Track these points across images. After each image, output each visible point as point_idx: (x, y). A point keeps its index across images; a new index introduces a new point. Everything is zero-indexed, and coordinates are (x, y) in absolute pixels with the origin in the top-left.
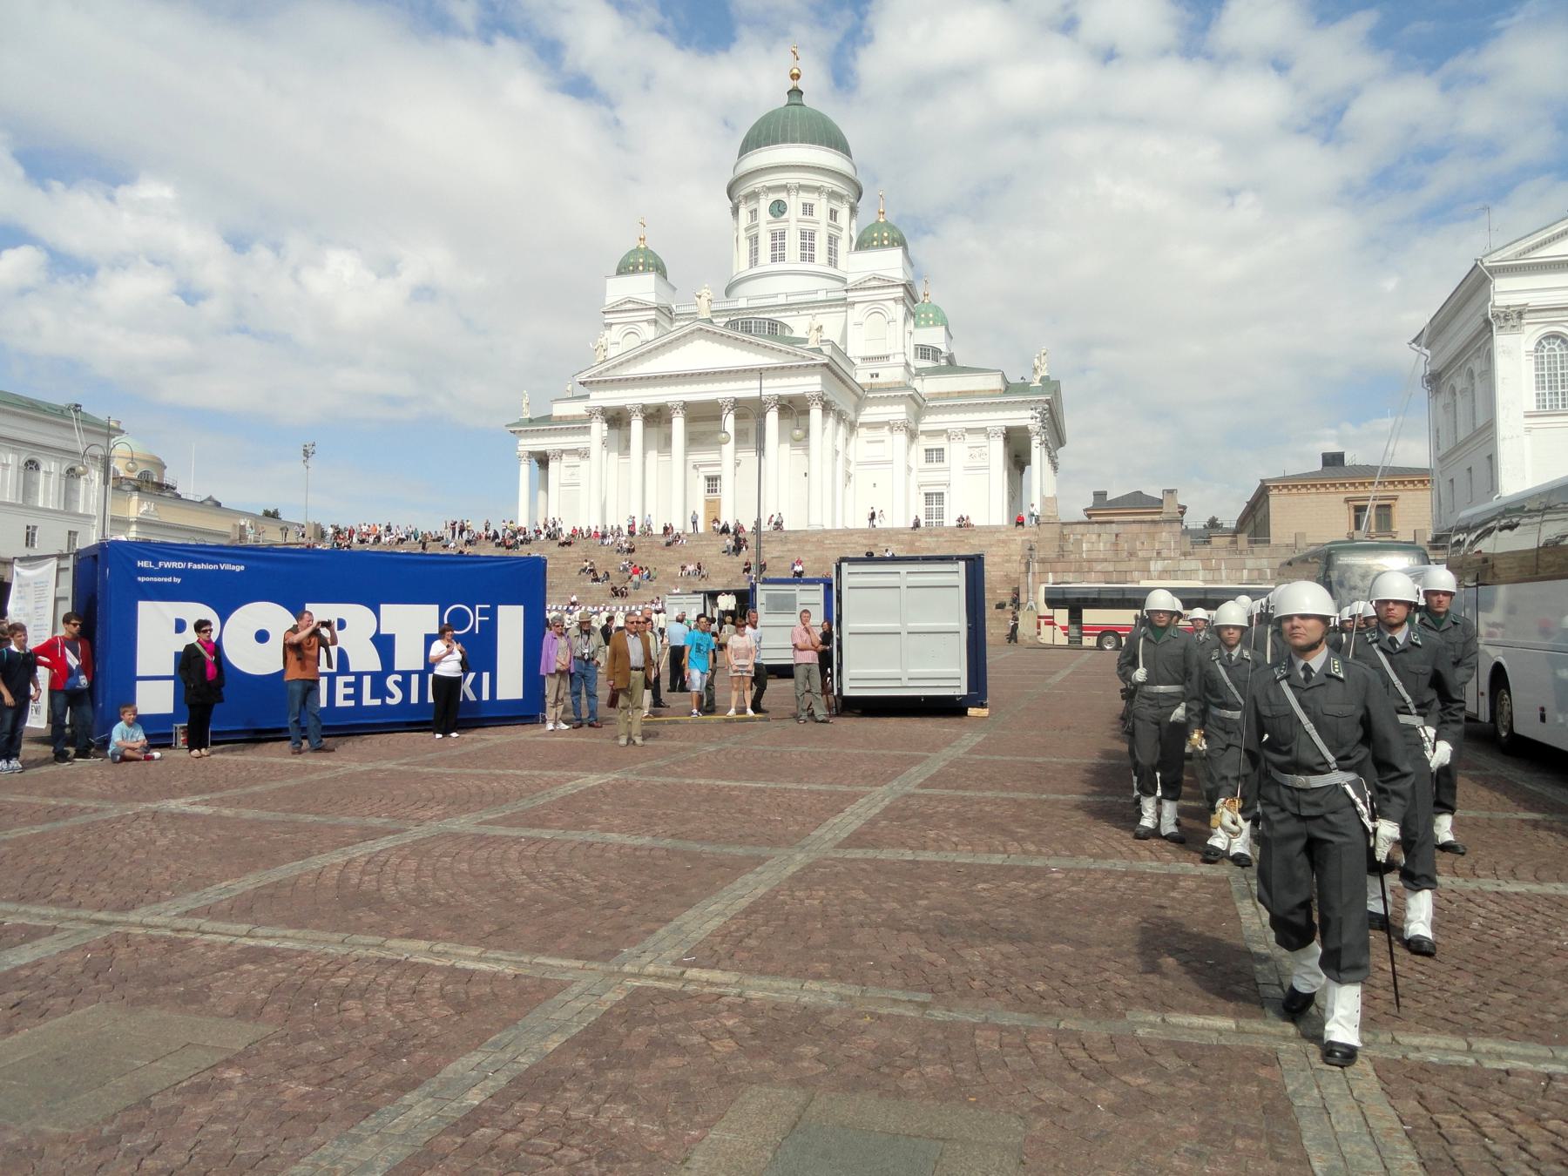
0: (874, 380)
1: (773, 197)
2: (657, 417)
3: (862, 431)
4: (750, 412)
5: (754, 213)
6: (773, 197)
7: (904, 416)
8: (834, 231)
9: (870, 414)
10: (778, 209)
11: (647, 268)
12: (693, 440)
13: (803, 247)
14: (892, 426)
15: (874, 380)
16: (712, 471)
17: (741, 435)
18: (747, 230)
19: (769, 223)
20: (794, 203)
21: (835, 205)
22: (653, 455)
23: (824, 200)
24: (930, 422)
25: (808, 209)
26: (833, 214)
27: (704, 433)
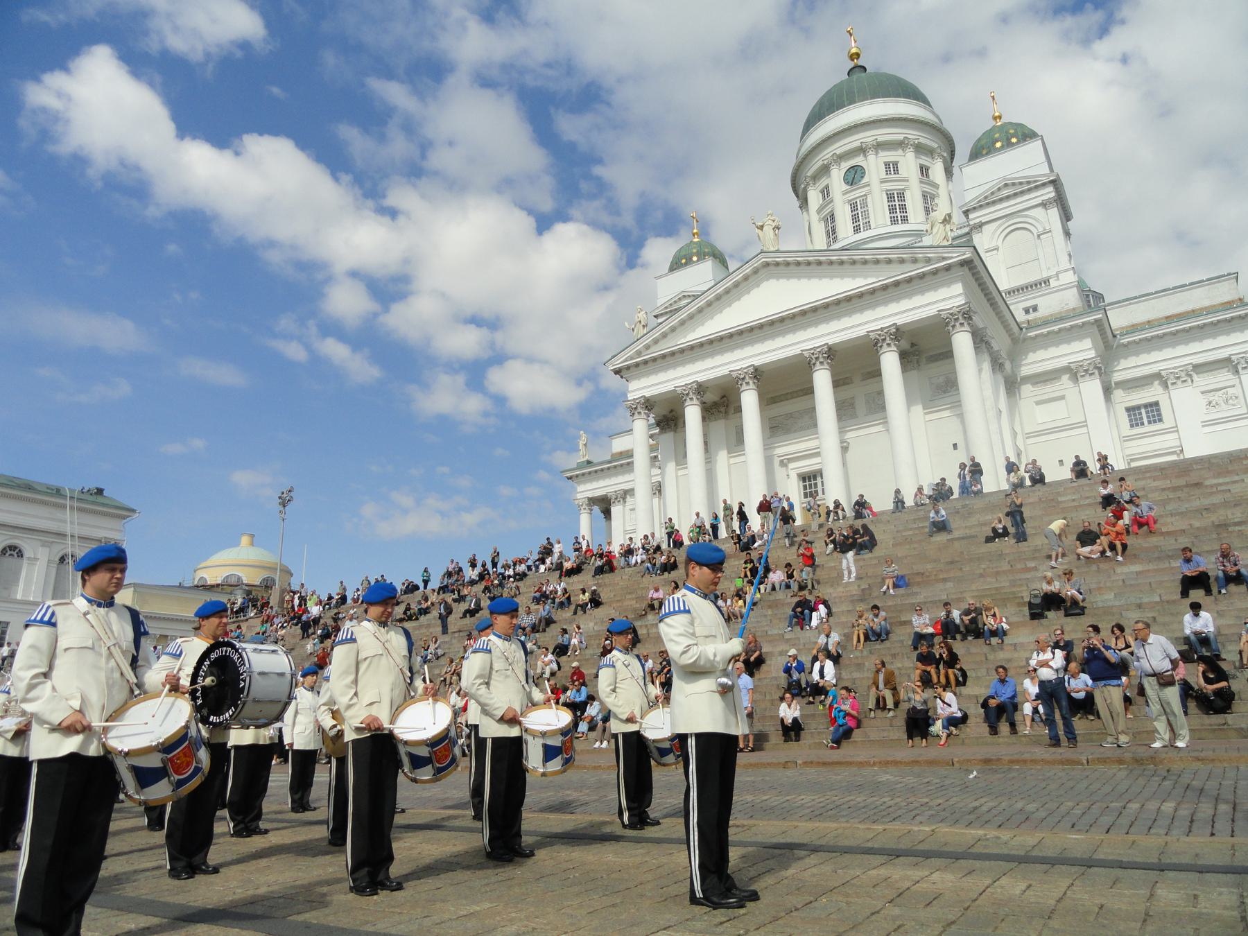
0: (1032, 316)
1: (846, 165)
2: (720, 403)
3: (1027, 389)
4: (855, 368)
5: (826, 191)
6: (846, 165)
7: (1092, 354)
8: (927, 188)
9: (1037, 361)
10: (854, 176)
11: (702, 256)
12: (775, 428)
13: (892, 209)
14: (1074, 373)
15: (1032, 316)
16: (807, 465)
17: (845, 410)
18: (819, 212)
19: (845, 193)
20: (874, 165)
21: (925, 161)
22: (722, 457)
23: (910, 154)
24: (1128, 367)
25: (892, 167)
26: (924, 171)
27: (790, 416)
